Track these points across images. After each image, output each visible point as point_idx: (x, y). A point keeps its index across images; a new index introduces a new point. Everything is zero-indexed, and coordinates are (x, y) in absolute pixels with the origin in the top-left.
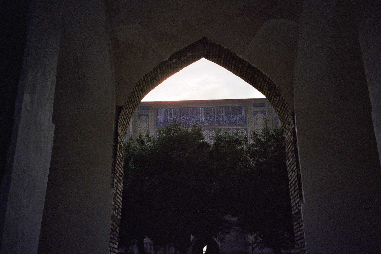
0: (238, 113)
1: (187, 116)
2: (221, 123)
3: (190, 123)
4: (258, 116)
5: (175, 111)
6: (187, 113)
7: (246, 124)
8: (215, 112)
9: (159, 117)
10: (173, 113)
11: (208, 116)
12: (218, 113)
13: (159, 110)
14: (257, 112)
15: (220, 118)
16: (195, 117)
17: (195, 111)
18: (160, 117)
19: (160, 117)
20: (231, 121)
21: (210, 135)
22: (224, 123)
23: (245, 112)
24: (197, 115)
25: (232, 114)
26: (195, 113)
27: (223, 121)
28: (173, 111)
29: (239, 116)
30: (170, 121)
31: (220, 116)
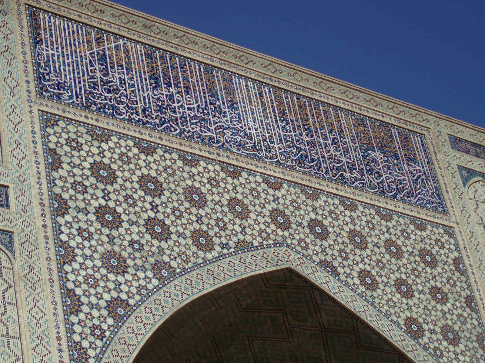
0: (401, 153)
2: (347, 175)
3: (209, 130)
5: (127, 51)
7: (445, 212)
8: (311, 120)
9: (46, 51)
12: (322, 128)
15: (337, 153)
16: (227, 110)
17: (219, 86)
18: (51, 52)
19: (51, 52)
20: (382, 182)
23: (426, 160)
24: (232, 105)
25: (381, 148)
26: (222, 94)
27: (352, 168)
28: (117, 47)
29: (411, 169)
30: (109, 92)
31: (334, 143)
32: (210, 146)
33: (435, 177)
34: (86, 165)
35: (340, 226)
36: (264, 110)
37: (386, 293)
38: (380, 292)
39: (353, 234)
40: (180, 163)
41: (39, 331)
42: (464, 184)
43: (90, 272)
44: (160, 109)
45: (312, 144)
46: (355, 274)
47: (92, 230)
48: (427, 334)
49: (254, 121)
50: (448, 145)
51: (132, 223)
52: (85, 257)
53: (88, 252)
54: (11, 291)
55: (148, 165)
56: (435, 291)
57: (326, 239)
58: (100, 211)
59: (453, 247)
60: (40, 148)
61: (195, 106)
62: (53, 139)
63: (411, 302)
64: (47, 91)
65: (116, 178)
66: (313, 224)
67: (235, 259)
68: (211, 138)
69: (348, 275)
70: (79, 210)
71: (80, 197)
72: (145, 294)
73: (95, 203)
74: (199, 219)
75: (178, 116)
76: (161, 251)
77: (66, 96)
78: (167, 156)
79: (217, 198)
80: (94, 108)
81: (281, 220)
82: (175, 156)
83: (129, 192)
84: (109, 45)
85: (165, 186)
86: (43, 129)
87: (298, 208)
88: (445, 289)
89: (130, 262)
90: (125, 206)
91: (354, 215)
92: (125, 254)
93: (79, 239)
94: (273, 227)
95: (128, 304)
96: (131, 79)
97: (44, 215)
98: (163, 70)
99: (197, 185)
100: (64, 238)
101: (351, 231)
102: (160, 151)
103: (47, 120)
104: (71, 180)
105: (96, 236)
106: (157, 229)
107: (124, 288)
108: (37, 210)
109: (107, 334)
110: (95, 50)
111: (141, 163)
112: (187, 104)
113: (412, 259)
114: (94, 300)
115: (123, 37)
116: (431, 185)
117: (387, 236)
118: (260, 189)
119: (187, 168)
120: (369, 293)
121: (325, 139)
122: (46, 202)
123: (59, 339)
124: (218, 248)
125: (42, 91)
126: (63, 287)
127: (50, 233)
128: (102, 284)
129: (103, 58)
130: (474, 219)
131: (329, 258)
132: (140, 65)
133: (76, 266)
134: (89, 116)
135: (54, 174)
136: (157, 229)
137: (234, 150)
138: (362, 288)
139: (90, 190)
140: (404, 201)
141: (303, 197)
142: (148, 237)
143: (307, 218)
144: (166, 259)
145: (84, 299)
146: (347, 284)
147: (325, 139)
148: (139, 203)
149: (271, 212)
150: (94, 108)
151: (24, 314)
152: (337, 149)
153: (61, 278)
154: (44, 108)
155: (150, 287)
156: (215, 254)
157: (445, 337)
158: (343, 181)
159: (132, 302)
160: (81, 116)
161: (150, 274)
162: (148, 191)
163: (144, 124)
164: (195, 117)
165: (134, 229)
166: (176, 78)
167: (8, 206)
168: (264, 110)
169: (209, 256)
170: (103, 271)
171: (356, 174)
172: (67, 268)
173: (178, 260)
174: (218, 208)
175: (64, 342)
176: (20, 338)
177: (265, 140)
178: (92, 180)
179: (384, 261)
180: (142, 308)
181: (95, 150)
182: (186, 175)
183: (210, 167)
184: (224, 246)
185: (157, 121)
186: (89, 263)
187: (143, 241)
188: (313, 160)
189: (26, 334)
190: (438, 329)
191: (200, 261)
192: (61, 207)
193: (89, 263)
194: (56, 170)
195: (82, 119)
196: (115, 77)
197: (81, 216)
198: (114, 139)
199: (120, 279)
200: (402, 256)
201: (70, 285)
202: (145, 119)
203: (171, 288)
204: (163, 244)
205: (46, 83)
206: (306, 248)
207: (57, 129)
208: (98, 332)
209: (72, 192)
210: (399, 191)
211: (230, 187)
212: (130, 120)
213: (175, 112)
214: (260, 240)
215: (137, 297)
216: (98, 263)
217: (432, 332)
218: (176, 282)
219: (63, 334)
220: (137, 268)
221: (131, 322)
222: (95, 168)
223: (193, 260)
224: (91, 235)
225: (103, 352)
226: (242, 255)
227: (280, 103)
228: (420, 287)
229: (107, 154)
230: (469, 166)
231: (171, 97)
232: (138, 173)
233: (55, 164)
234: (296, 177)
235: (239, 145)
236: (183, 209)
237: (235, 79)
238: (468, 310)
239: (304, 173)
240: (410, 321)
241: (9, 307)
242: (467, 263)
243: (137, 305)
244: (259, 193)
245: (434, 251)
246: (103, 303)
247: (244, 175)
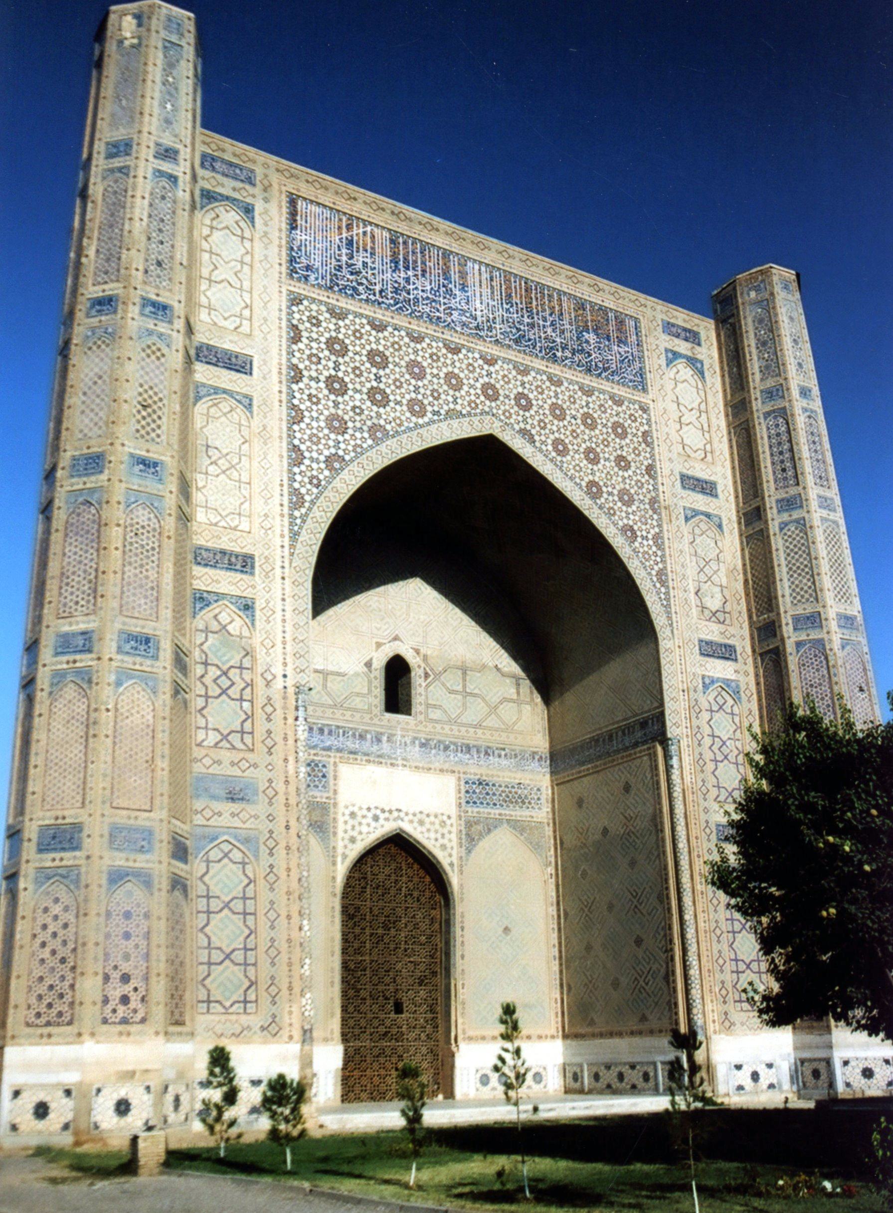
0: (614, 335)
1: (423, 275)
2: (559, 354)
4: (681, 373)
5: (373, 237)
6: (423, 263)
7: (645, 390)
8: (534, 303)
10: (365, 245)
11: (507, 310)
12: (544, 310)
13: (300, 204)
14: (676, 355)
21: (520, 390)
22: (566, 358)
25: (595, 331)
26: (455, 276)
27: (564, 348)
28: (365, 233)
30: (352, 274)
31: (552, 324)
32: (437, 325)
33: (641, 359)
34: (323, 340)
35: (542, 402)
36: (493, 293)
37: (575, 459)
38: (569, 458)
39: (554, 407)
40: (406, 340)
41: (266, 479)
42: (668, 365)
43: (315, 431)
44: (396, 291)
45: (532, 326)
46: (549, 442)
47: (320, 396)
48: (605, 495)
49: (481, 302)
50: (660, 329)
51: (356, 391)
52: (312, 418)
53: (315, 414)
54: (247, 445)
55: (378, 341)
56: (620, 459)
57: (528, 410)
58: (330, 380)
59: (644, 421)
60: (284, 323)
61: (429, 288)
62: (297, 316)
63: (595, 468)
64: (296, 273)
65: (347, 350)
66: (520, 396)
67: (444, 425)
68: (439, 318)
69: (543, 443)
70: (311, 378)
71: (314, 367)
72: (359, 451)
73: (326, 373)
74: (417, 389)
75: (412, 297)
76: (379, 416)
77: (312, 277)
78: (396, 333)
79: (435, 371)
80: (336, 288)
81: (490, 392)
82: (403, 333)
83: (358, 364)
84: (358, 231)
85: (390, 359)
86: (289, 307)
87: (508, 383)
88: (629, 458)
89: (350, 424)
90: (352, 376)
91: (559, 390)
92: (346, 417)
93: (308, 404)
94: (482, 398)
95: (344, 460)
96: (373, 263)
97: (280, 382)
98: (402, 254)
99: (419, 359)
100: (296, 402)
101: (553, 404)
102: (390, 329)
103: (295, 299)
104: (308, 352)
105: (323, 402)
106: (378, 397)
107: (342, 446)
108: (275, 377)
109: (323, 483)
110: (344, 235)
111: (372, 339)
112: (422, 287)
113: (605, 430)
114: (315, 455)
115: (371, 223)
116: (637, 365)
117: (585, 409)
118: (476, 365)
119: (412, 345)
120: (559, 458)
121: (545, 320)
122: (284, 372)
123: (282, 485)
124: (429, 415)
125: (292, 272)
126: (290, 443)
127: (284, 397)
128: (323, 441)
129: (350, 243)
130: (671, 396)
131: (528, 427)
132: (384, 249)
133: (303, 425)
134: (331, 296)
135: (294, 347)
136: (378, 397)
137: (458, 329)
138: (554, 454)
139: (323, 362)
140: (608, 380)
141: (514, 373)
142: (368, 403)
143: (515, 391)
144: (382, 422)
145: (307, 454)
146: (541, 451)
147: (545, 320)
148: (365, 374)
149: (483, 385)
150: (336, 288)
151: (255, 464)
152: (554, 331)
153: (289, 436)
154: (292, 289)
155: (365, 446)
156: (426, 419)
157: (621, 499)
158: (554, 359)
159: (347, 458)
160: (322, 295)
161: (366, 435)
162: (374, 364)
163: (379, 304)
164: (428, 298)
165: (358, 396)
166: (415, 262)
167: (251, 374)
168: (493, 293)
169: (421, 421)
170: (326, 431)
171: (568, 354)
172: (296, 427)
173: (393, 424)
174: (435, 380)
175: (285, 488)
176: (249, 483)
177: (488, 321)
178: (327, 353)
179: (579, 431)
180: (355, 463)
181: (332, 327)
182: (410, 350)
183: (434, 344)
184: (435, 413)
185: (392, 302)
186: (315, 424)
187: (364, 407)
188: (530, 340)
189: (255, 481)
190: (616, 492)
191: (412, 425)
192: (296, 376)
193: (315, 424)
194: (295, 343)
195: (325, 299)
196: (359, 260)
197: (313, 384)
198: (351, 317)
199: (340, 438)
200: (596, 427)
201: (296, 442)
202: (380, 300)
203: (383, 447)
204: (382, 410)
205: (296, 266)
206: (509, 418)
207: (301, 307)
208: (315, 481)
209: (307, 363)
210: (605, 369)
211: (448, 362)
212: (367, 300)
213: (409, 294)
214: (468, 409)
215: (352, 454)
216: (323, 424)
217: (610, 494)
218: (388, 443)
219: (286, 482)
220: (355, 429)
221: (344, 474)
222: (330, 342)
223: (406, 424)
224: (319, 400)
225: (317, 498)
226: (451, 422)
227: (509, 288)
228: (607, 455)
229: (343, 330)
230: (676, 349)
231: (407, 280)
232: (368, 348)
233: (296, 338)
234: (511, 355)
235: (464, 325)
236: (403, 380)
237: (470, 264)
238: (647, 477)
239: (519, 351)
240: (592, 484)
241: (243, 458)
242: (655, 436)
243: (352, 461)
244: (474, 368)
245: (626, 425)
246: (322, 458)
247: (464, 351)
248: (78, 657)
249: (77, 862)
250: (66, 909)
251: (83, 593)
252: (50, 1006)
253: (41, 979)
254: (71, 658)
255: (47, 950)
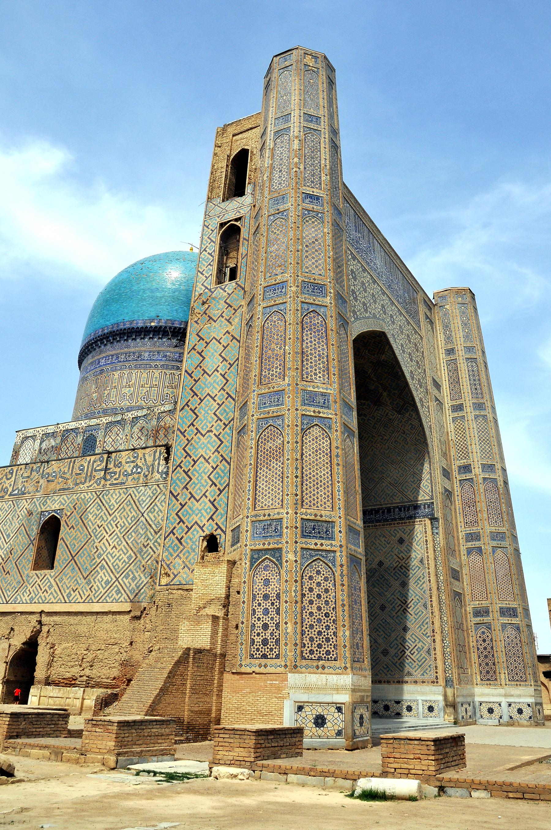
248: (321, 410)
249: (333, 549)
250: (326, 579)
251: (320, 368)
252: (320, 646)
253: (312, 626)
254: (317, 410)
255: (315, 606)
